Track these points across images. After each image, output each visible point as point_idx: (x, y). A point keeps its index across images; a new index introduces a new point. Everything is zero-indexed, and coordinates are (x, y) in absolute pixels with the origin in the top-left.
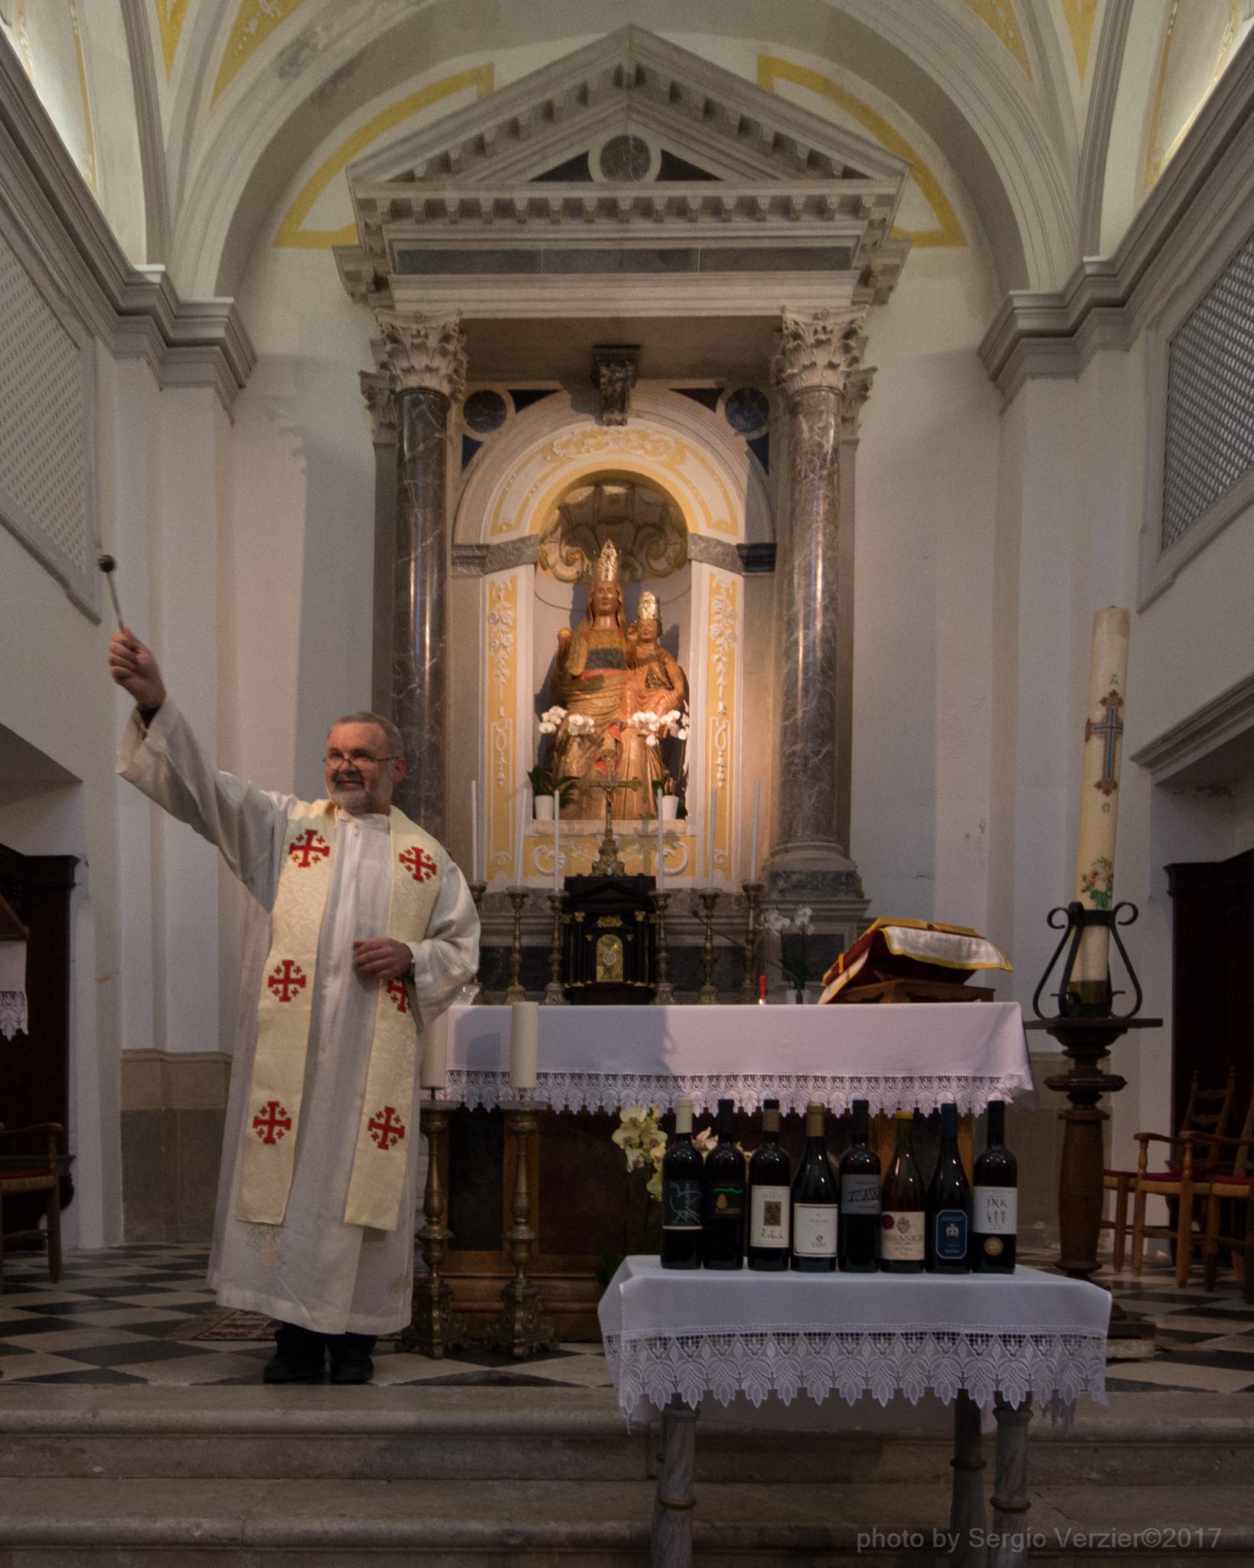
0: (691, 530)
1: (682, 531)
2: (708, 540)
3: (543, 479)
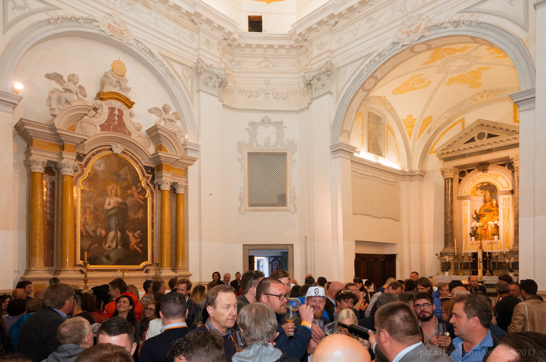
0: (498, 190)
1: (497, 190)
2: (502, 191)
3: (472, 185)
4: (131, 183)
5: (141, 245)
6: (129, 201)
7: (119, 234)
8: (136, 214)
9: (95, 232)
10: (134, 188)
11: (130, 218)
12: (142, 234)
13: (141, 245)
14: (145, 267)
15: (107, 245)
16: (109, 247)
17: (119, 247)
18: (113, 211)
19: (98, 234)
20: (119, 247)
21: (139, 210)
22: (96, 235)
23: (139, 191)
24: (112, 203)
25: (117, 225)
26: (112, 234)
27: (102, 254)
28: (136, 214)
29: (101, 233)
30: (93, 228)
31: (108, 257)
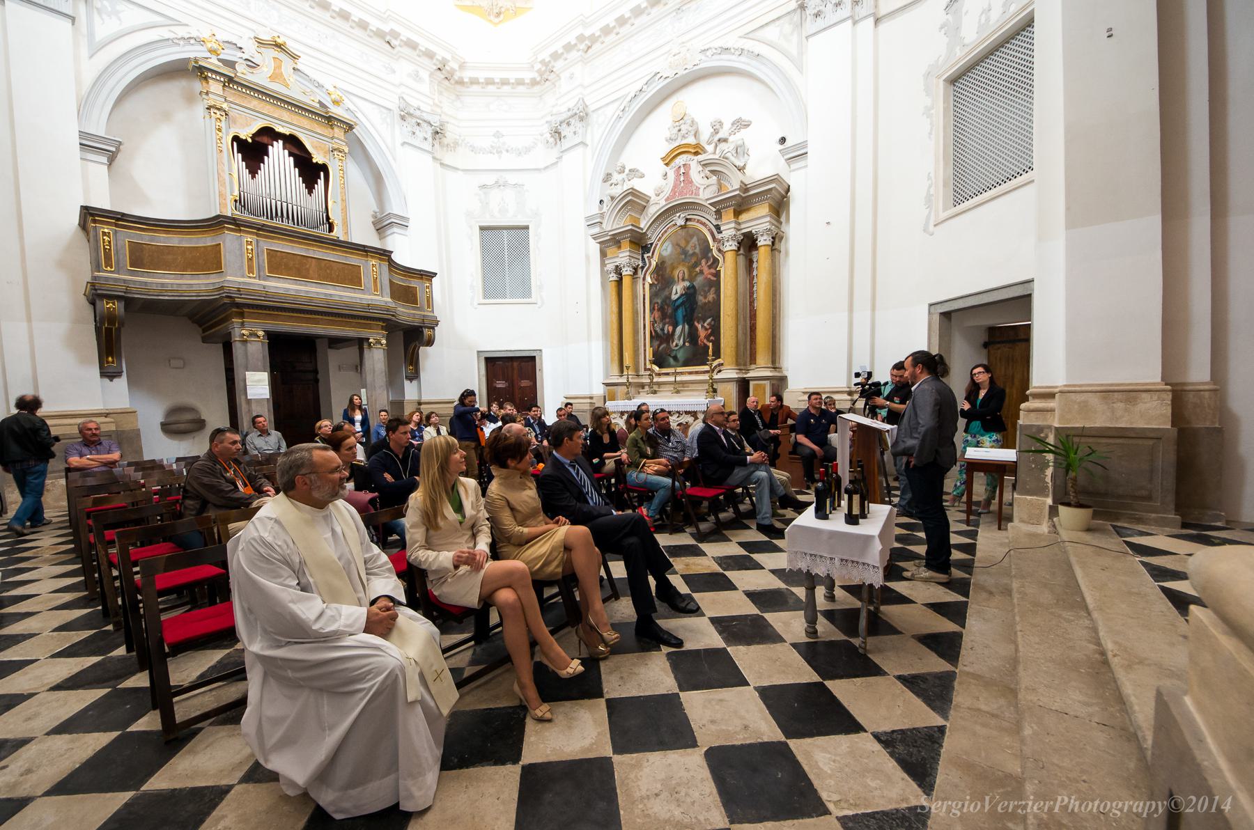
4: (700, 256)
5: (712, 338)
6: (699, 281)
7: (687, 327)
8: (705, 298)
9: (662, 330)
10: (703, 262)
11: (699, 303)
12: (713, 323)
13: (712, 338)
14: (716, 367)
15: (674, 344)
16: (677, 345)
17: (687, 344)
18: (681, 300)
19: (666, 332)
20: (687, 344)
21: (709, 290)
22: (664, 333)
23: (709, 263)
24: (679, 291)
25: (684, 317)
26: (679, 329)
27: (669, 355)
28: (705, 298)
29: (668, 331)
30: (661, 326)
31: (675, 358)
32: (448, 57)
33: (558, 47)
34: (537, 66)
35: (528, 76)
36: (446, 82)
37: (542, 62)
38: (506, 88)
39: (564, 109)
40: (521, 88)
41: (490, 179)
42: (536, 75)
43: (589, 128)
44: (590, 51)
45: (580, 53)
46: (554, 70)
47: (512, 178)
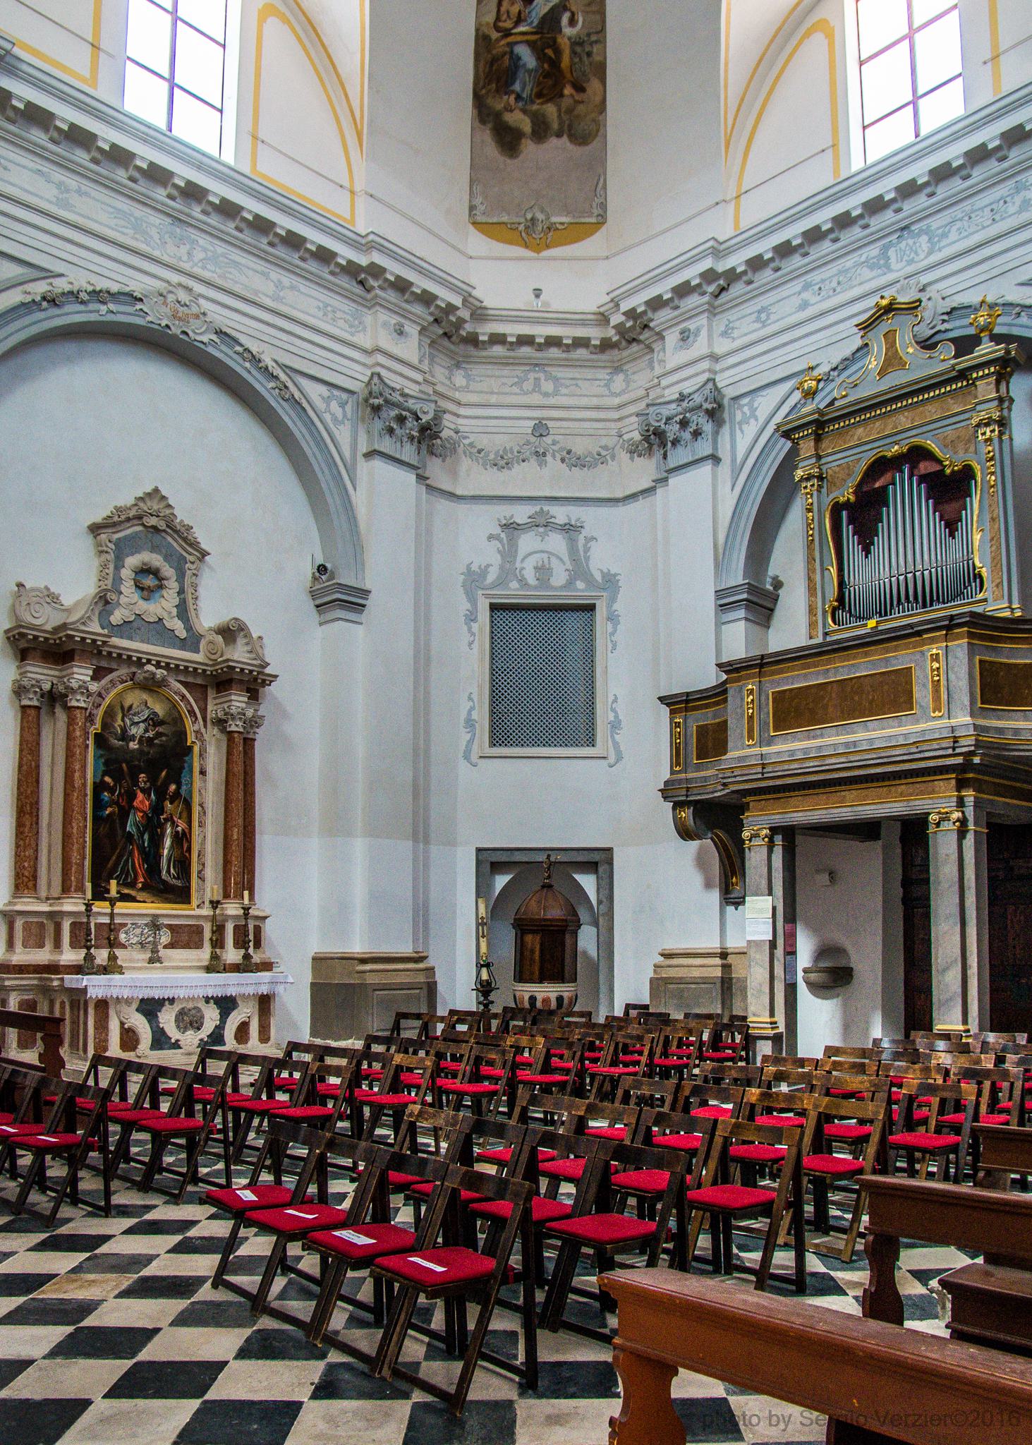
32: (457, 301)
33: (663, 289)
34: (616, 319)
35: (595, 334)
36: (446, 342)
37: (631, 314)
38: (554, 352)
39: (672, 394)
40: (581, 353)
41: (521, 514)
42: (611, 333)
43: (726, 430)
44: (723, 294)
45: (706, 298)
46: (652, 325)
47: (560, 514)
